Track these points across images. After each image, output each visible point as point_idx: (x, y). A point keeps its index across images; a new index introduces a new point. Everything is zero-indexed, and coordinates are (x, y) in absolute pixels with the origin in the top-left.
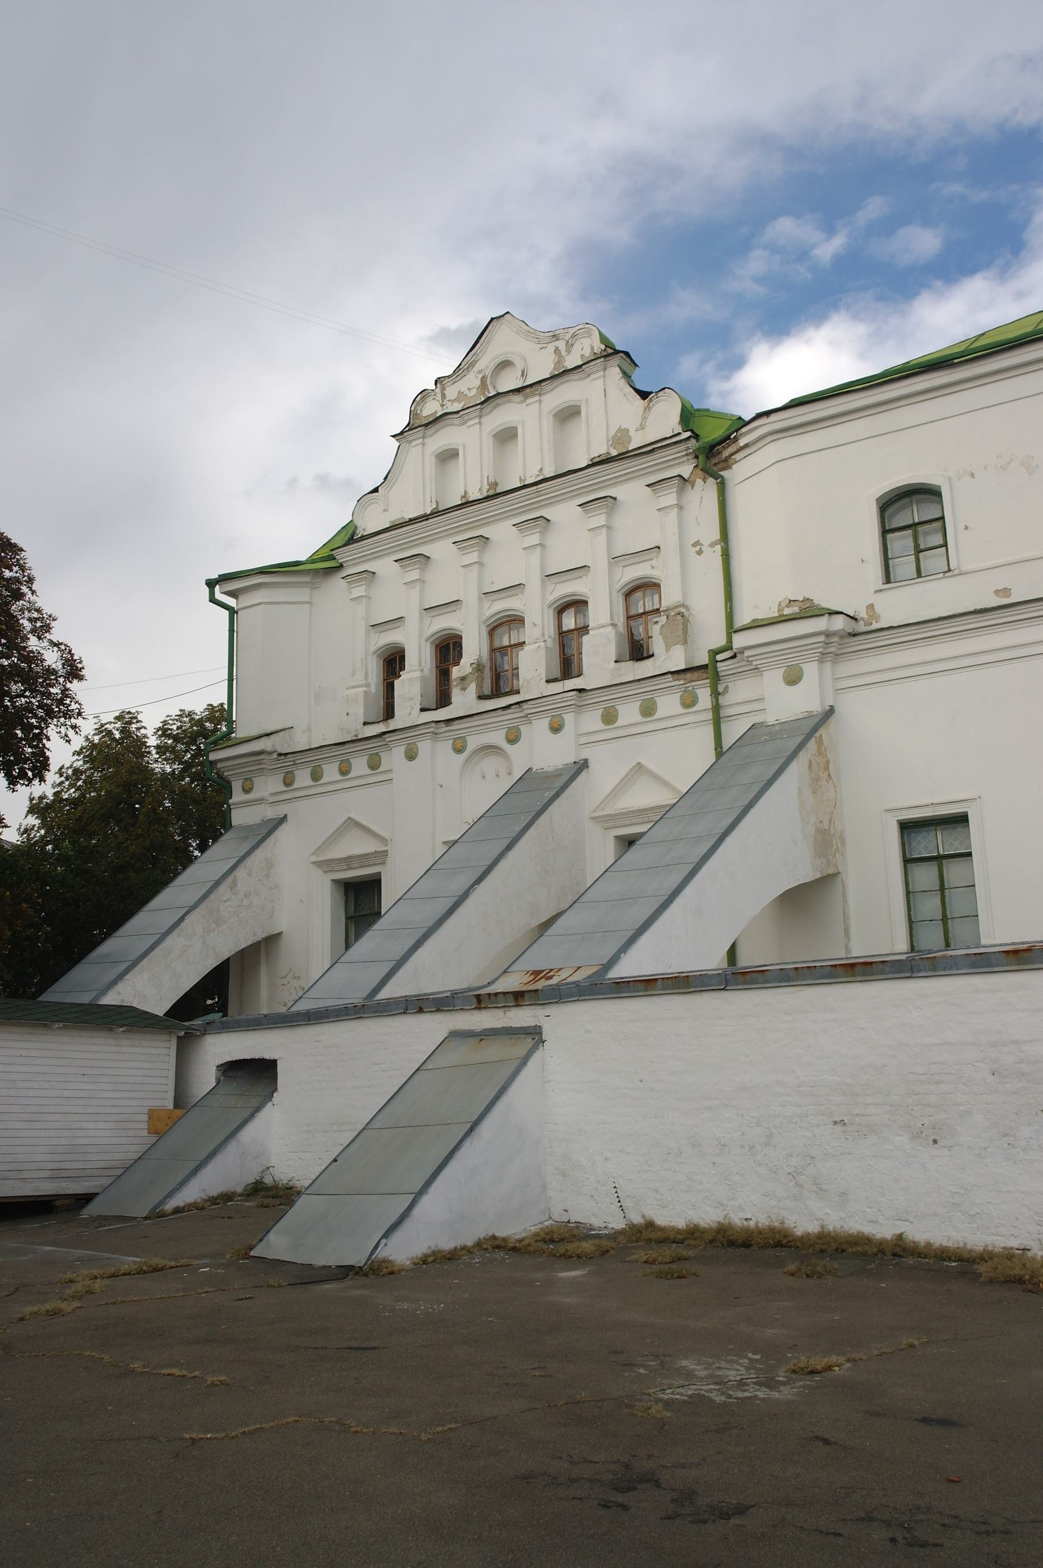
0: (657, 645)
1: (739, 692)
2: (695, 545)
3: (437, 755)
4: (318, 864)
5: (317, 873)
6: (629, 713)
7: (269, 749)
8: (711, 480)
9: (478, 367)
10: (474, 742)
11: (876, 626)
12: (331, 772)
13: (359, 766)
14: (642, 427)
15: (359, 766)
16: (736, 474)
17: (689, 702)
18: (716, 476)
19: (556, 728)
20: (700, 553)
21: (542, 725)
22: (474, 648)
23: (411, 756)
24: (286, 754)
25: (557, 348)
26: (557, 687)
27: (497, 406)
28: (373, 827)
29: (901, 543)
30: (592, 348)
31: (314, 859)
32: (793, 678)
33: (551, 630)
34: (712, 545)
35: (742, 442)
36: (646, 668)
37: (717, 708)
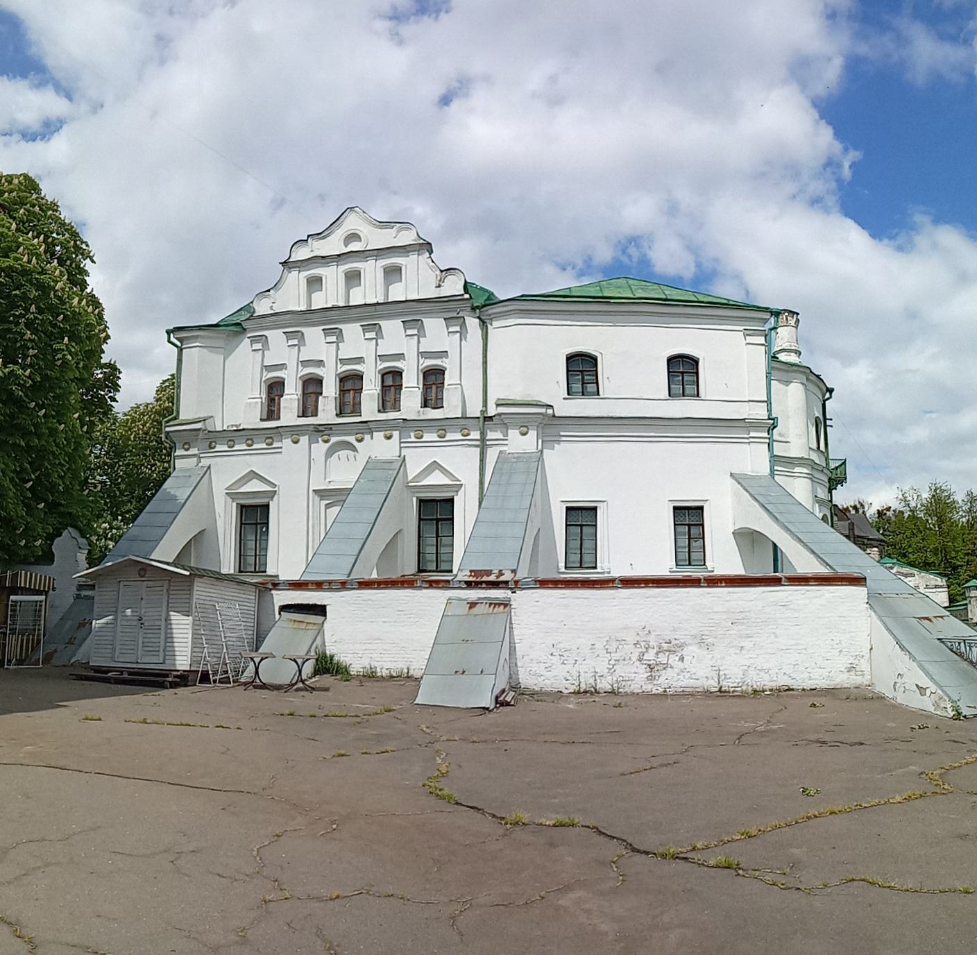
26: (383, 416)
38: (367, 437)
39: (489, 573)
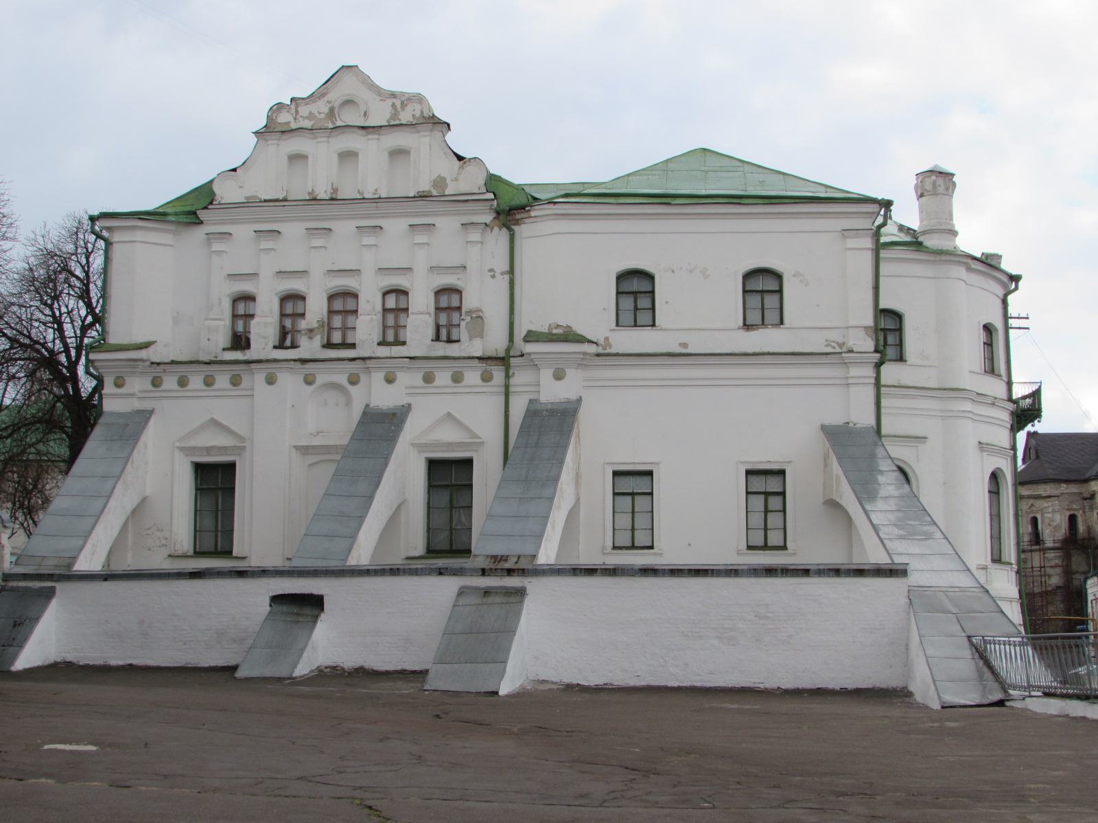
0: (464, 336)
1: (520, 378)
2: (491, 270)
3: (289, 381)
4: (181, 449)
5: (179, 456)
6: (443, 378)
7: (145, 358)
8: (504, 230)
9: (330, 97)
10: (321, 379)
11: (608, 351)
12: (196, 382)
13: (222, 381)
14: (456, 179)
15: (222, 381)
16: (523, 231)
17: (487, 378)
18: (510, 229)
19: (390, 380)
20: (493, 277)
21: (378, 377)
22: (316, 308)
23: (271, 381)
24: (158, 364)
25: (394, 104)
26: (384, 351)
27: (343, 132)
28: (233, 428)
29: (628, 303)
30: (422, 112)
31: (177, 444)
32: (559, 376)
33: (379, 308)
34: (502, 274)
35: (533, 214)
36: (453, 350)
37: (507, 387)
38: (363, 378)
39: (504, 558)
